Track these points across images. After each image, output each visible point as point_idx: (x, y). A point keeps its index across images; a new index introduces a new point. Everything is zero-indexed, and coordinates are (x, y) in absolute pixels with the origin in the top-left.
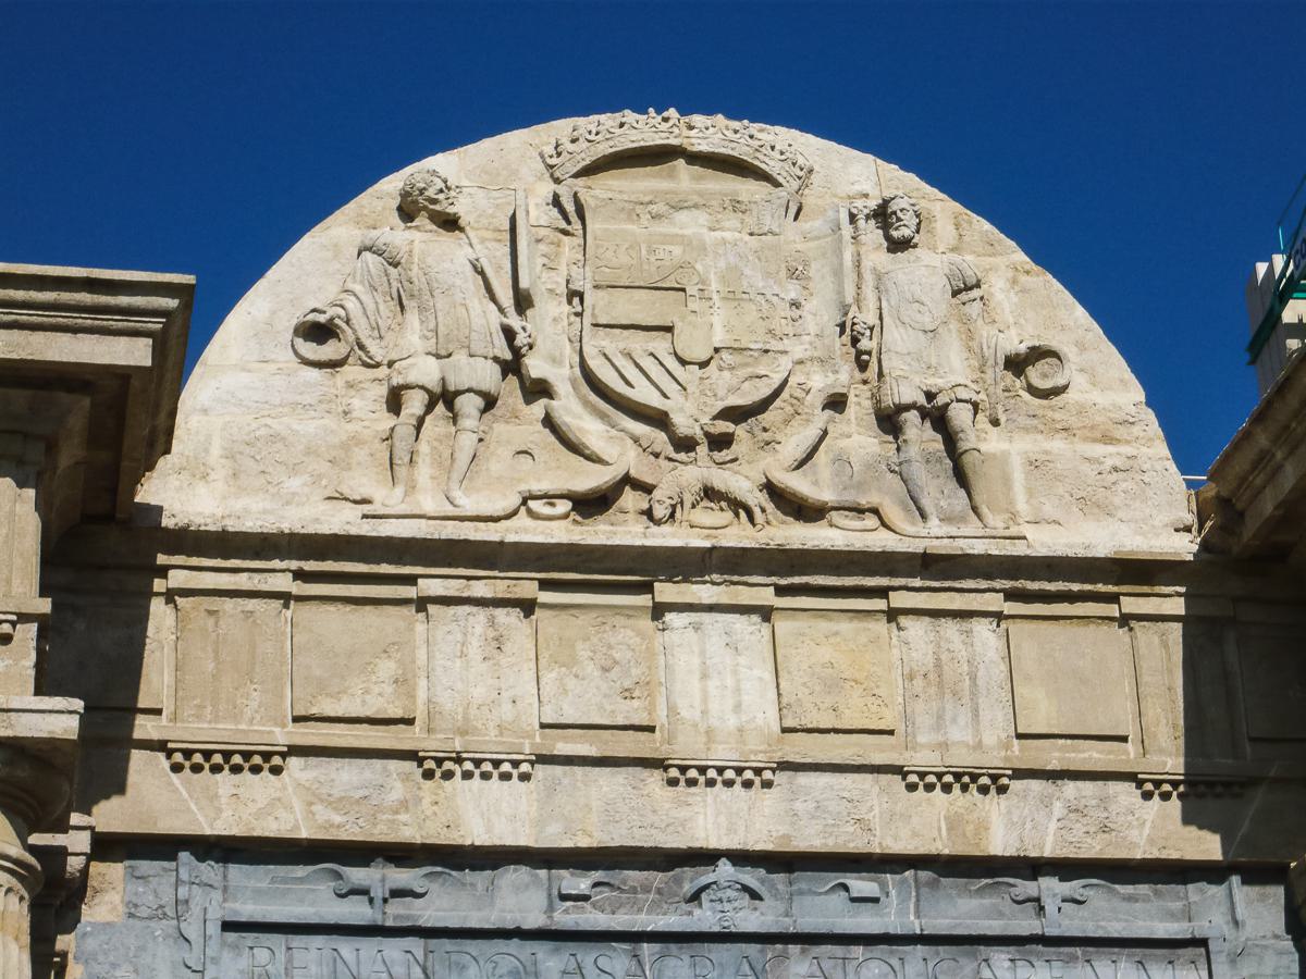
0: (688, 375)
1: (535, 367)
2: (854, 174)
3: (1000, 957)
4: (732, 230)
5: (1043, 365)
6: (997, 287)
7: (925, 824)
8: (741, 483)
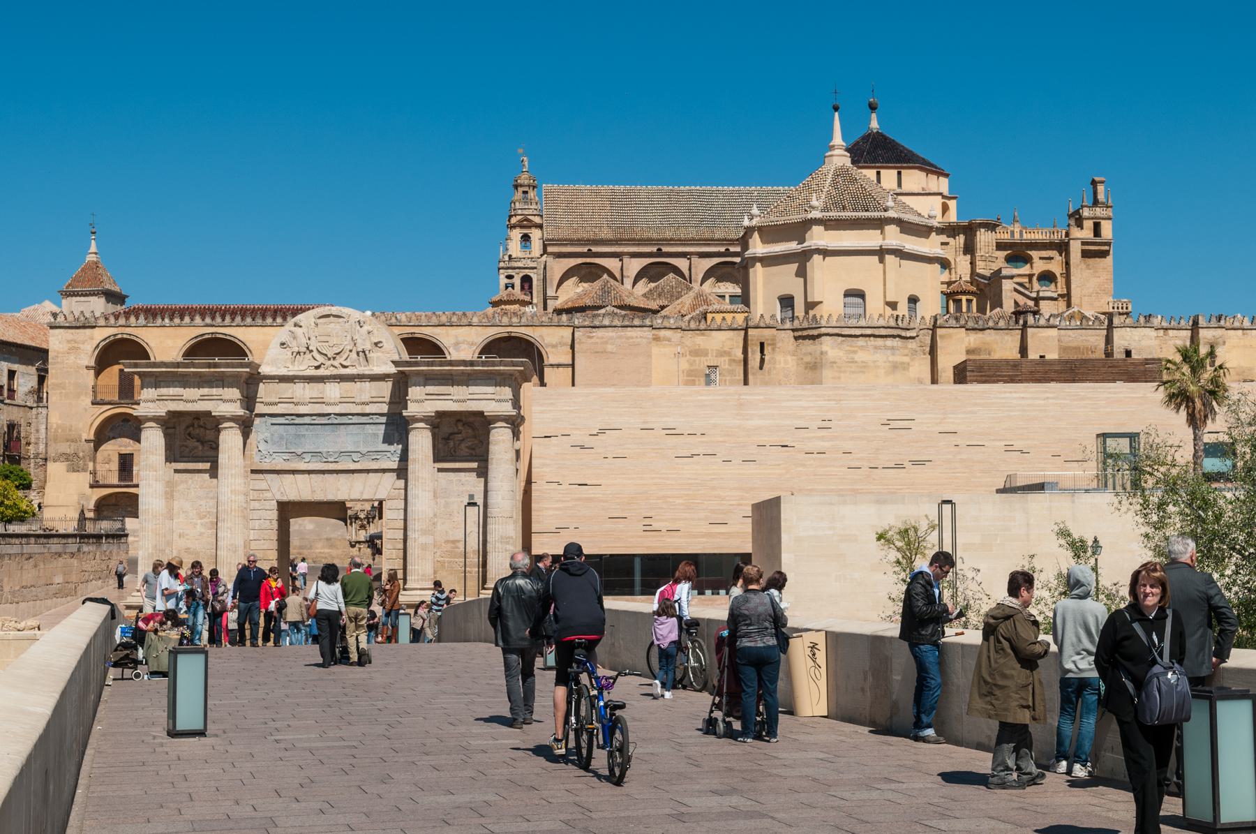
2: (355, 314)
4: (338, 326)
7: (358, 409)
8: (336, 363)
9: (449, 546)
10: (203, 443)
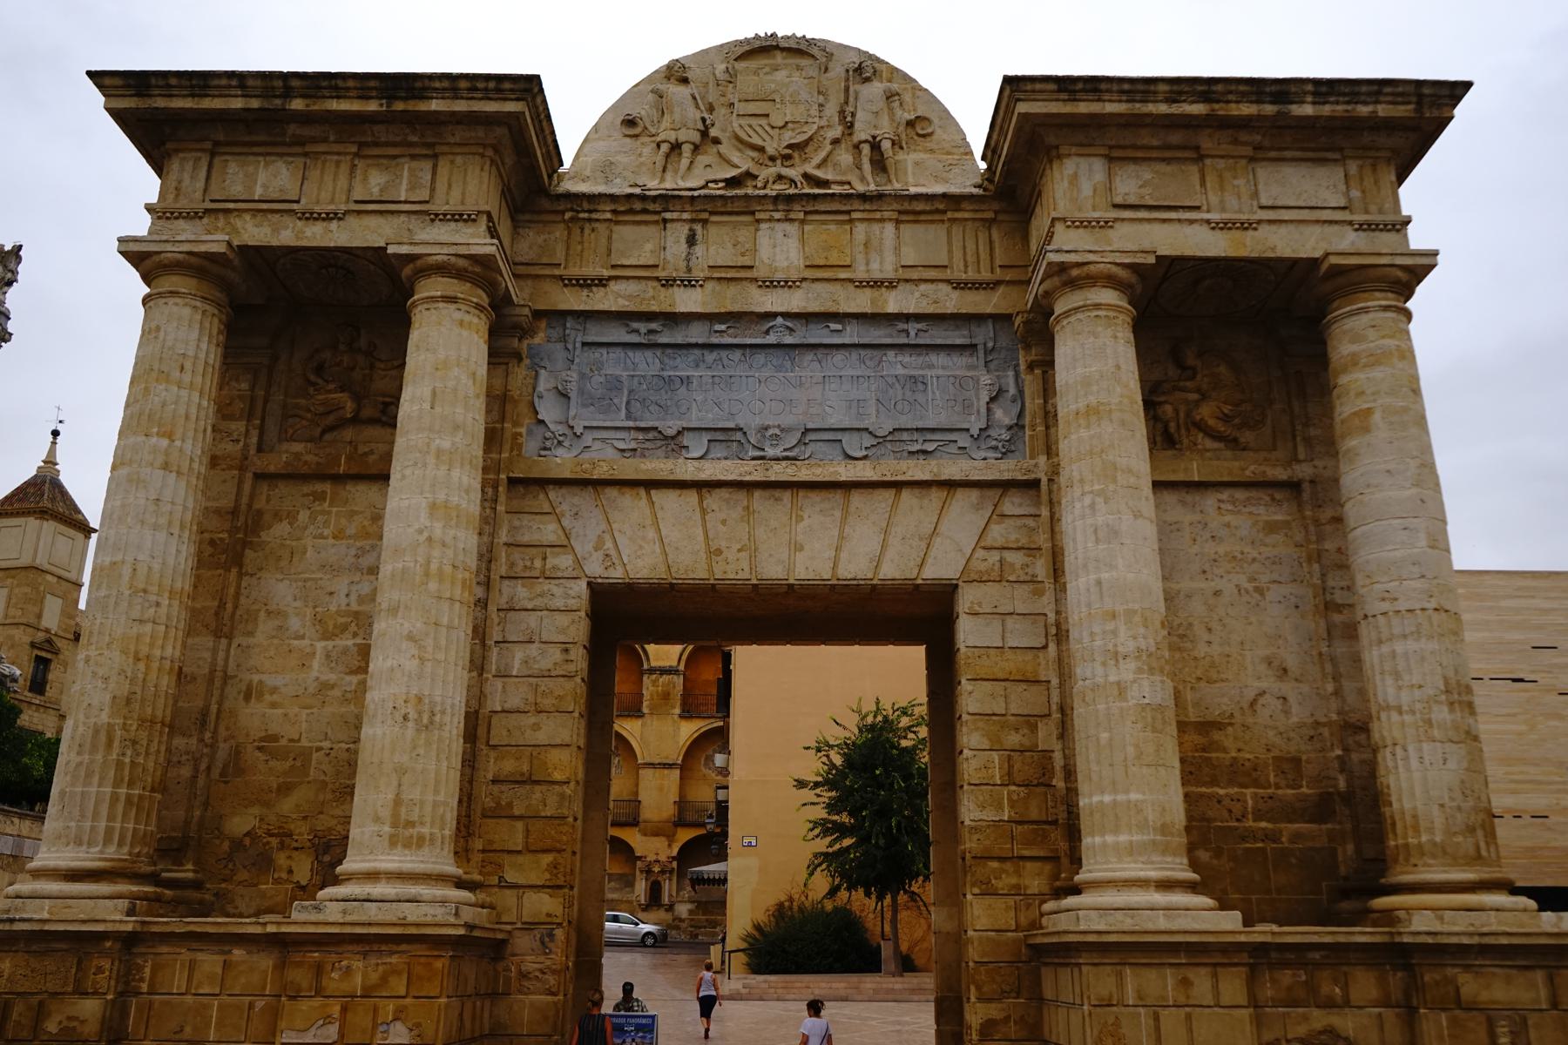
0: (775, 133)
1: (713, 132)
3: (891, 353)
4: (796, 76)
5: (925, 124)
6: (907, 97)
7: (861, 302)
10: (358, 398)
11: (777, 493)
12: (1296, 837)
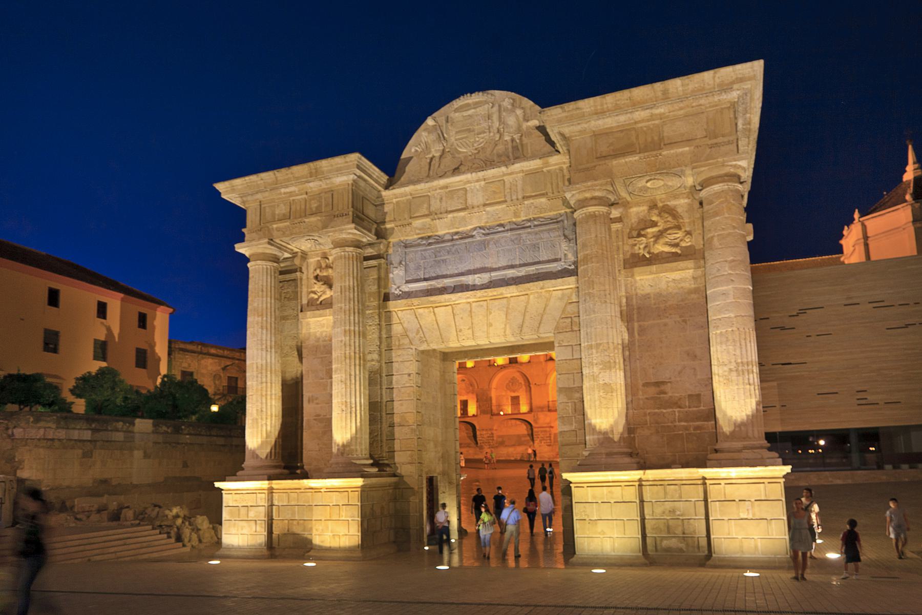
9: (652, 391)
11: (481, 303)
12: (697, 428)
